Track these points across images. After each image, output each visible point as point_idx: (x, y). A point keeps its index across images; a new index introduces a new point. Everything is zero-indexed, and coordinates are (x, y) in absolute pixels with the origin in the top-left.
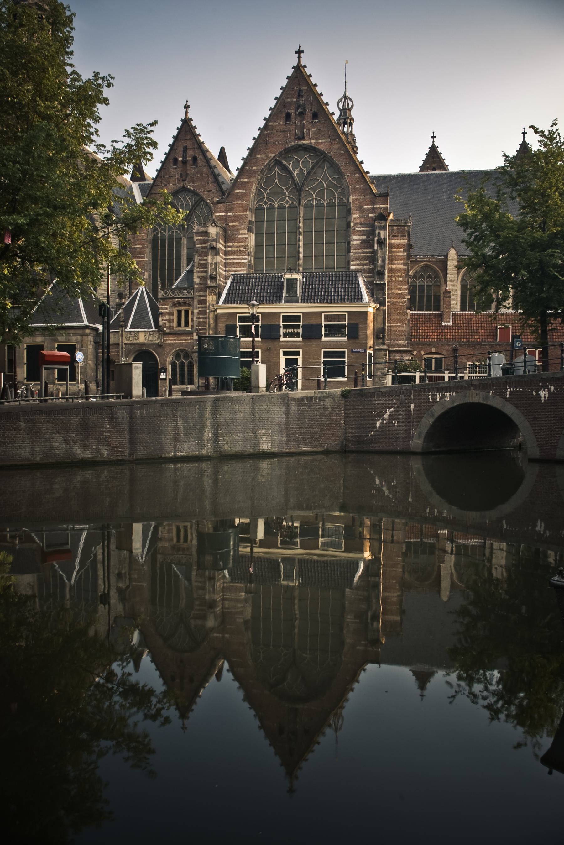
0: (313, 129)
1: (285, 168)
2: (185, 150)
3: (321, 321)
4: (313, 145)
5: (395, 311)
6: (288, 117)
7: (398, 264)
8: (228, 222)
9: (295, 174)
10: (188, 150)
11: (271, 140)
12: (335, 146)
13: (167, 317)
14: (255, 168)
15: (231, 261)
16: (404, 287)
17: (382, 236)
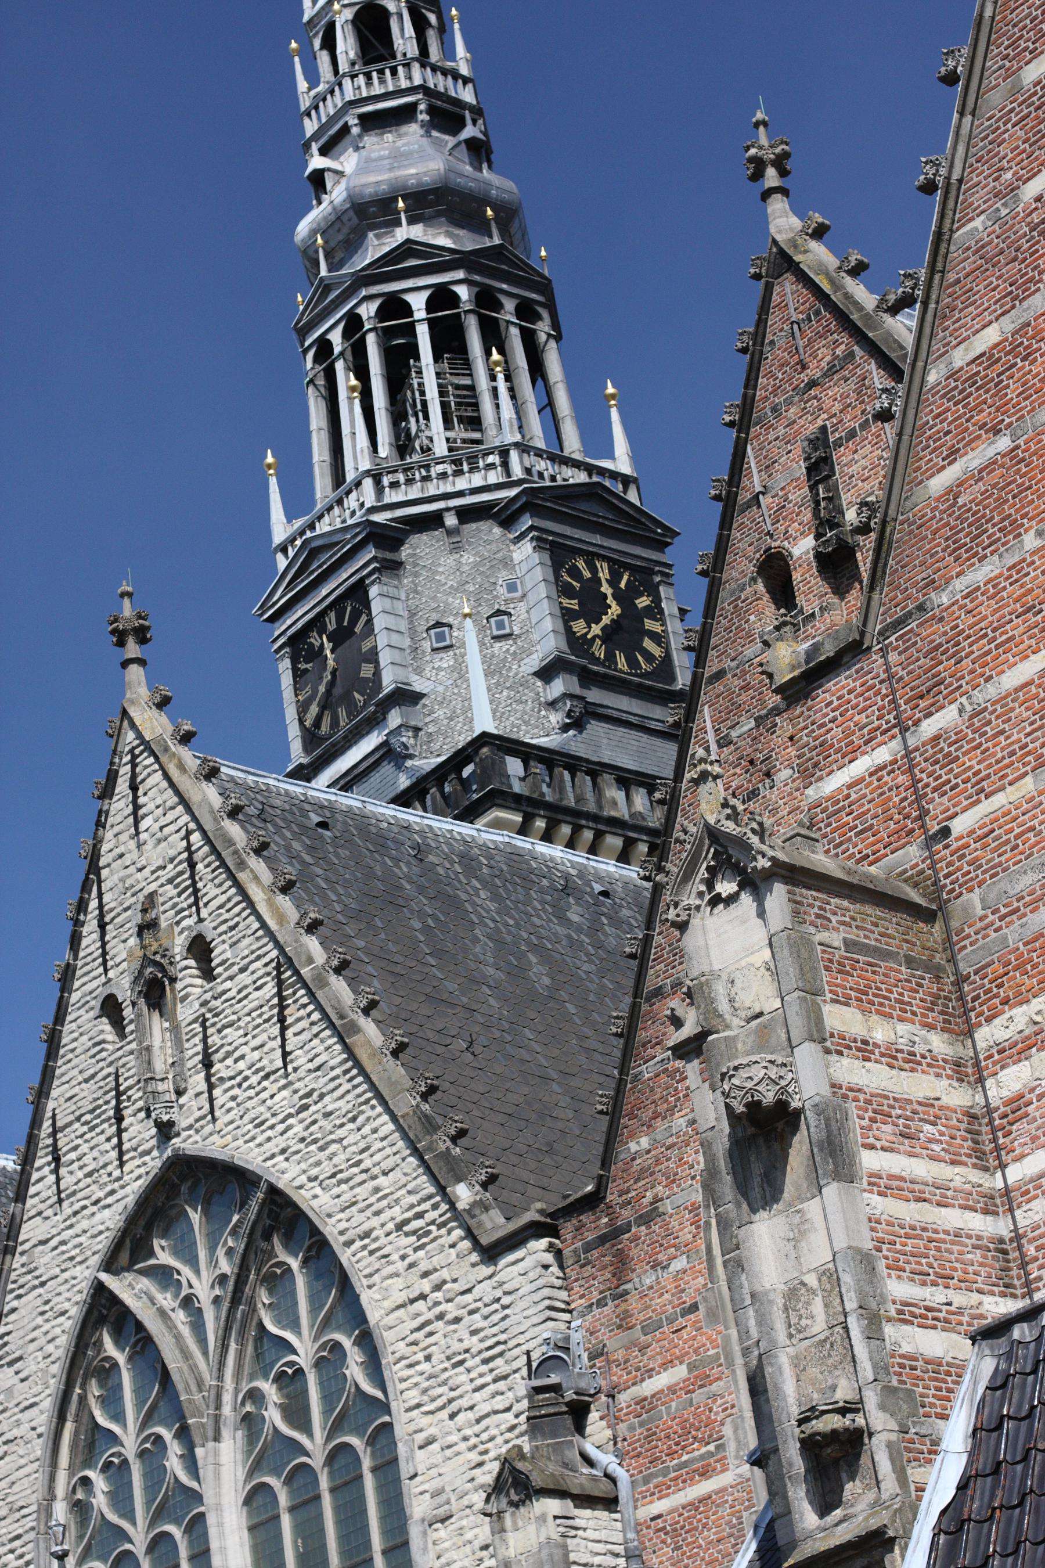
8: (938, 804)
10: (841, 457)
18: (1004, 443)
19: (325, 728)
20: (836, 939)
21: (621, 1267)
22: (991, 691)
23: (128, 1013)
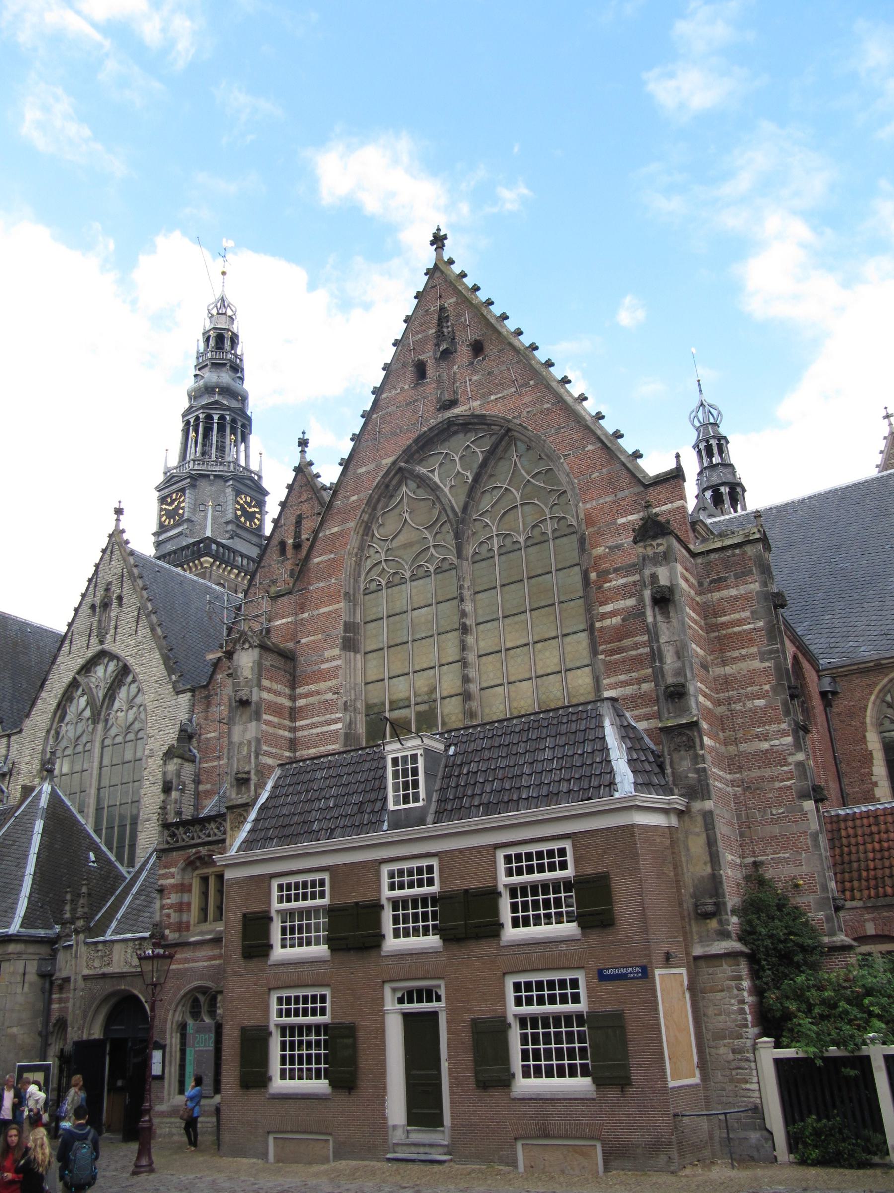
0: (475, 378)
1: (423, 482)
2: (299, 522)
3: (495, 878)
4: (477, 412)
5: (763, 810)
6: (421, 370)
7: (743, 658)
8: (299, 635)
9: (447, 490)
10: (304, 522)
11: (386, 429)
12: (527, 399)
13: (173, 899)
14: (354, 498)
15: (306, 733)
16: (775, 727)
17: (663, 581)
18: (332, 556)
19: (167, 523)
20: (268, 663)
21: (208, 705)
22: (317, 612)
23: (98, 610)
